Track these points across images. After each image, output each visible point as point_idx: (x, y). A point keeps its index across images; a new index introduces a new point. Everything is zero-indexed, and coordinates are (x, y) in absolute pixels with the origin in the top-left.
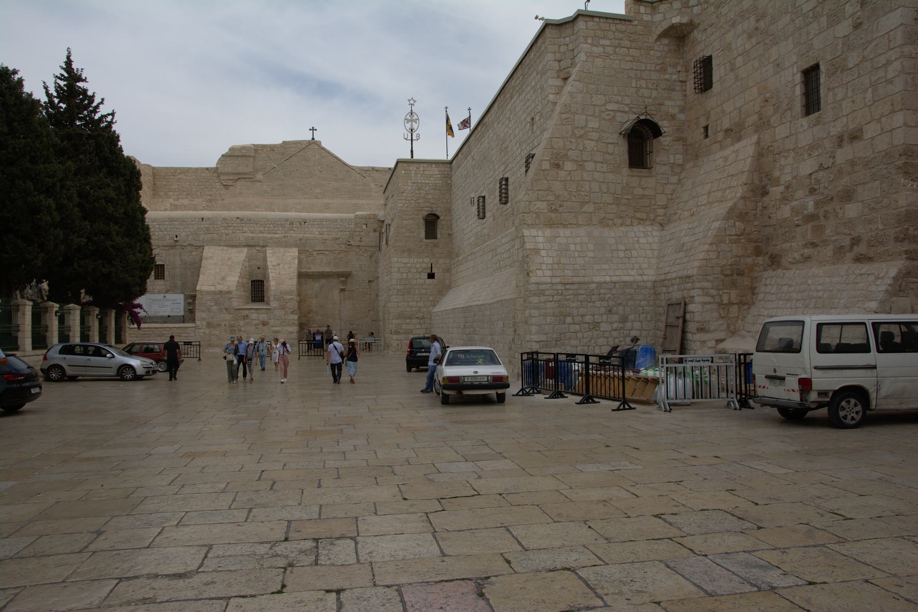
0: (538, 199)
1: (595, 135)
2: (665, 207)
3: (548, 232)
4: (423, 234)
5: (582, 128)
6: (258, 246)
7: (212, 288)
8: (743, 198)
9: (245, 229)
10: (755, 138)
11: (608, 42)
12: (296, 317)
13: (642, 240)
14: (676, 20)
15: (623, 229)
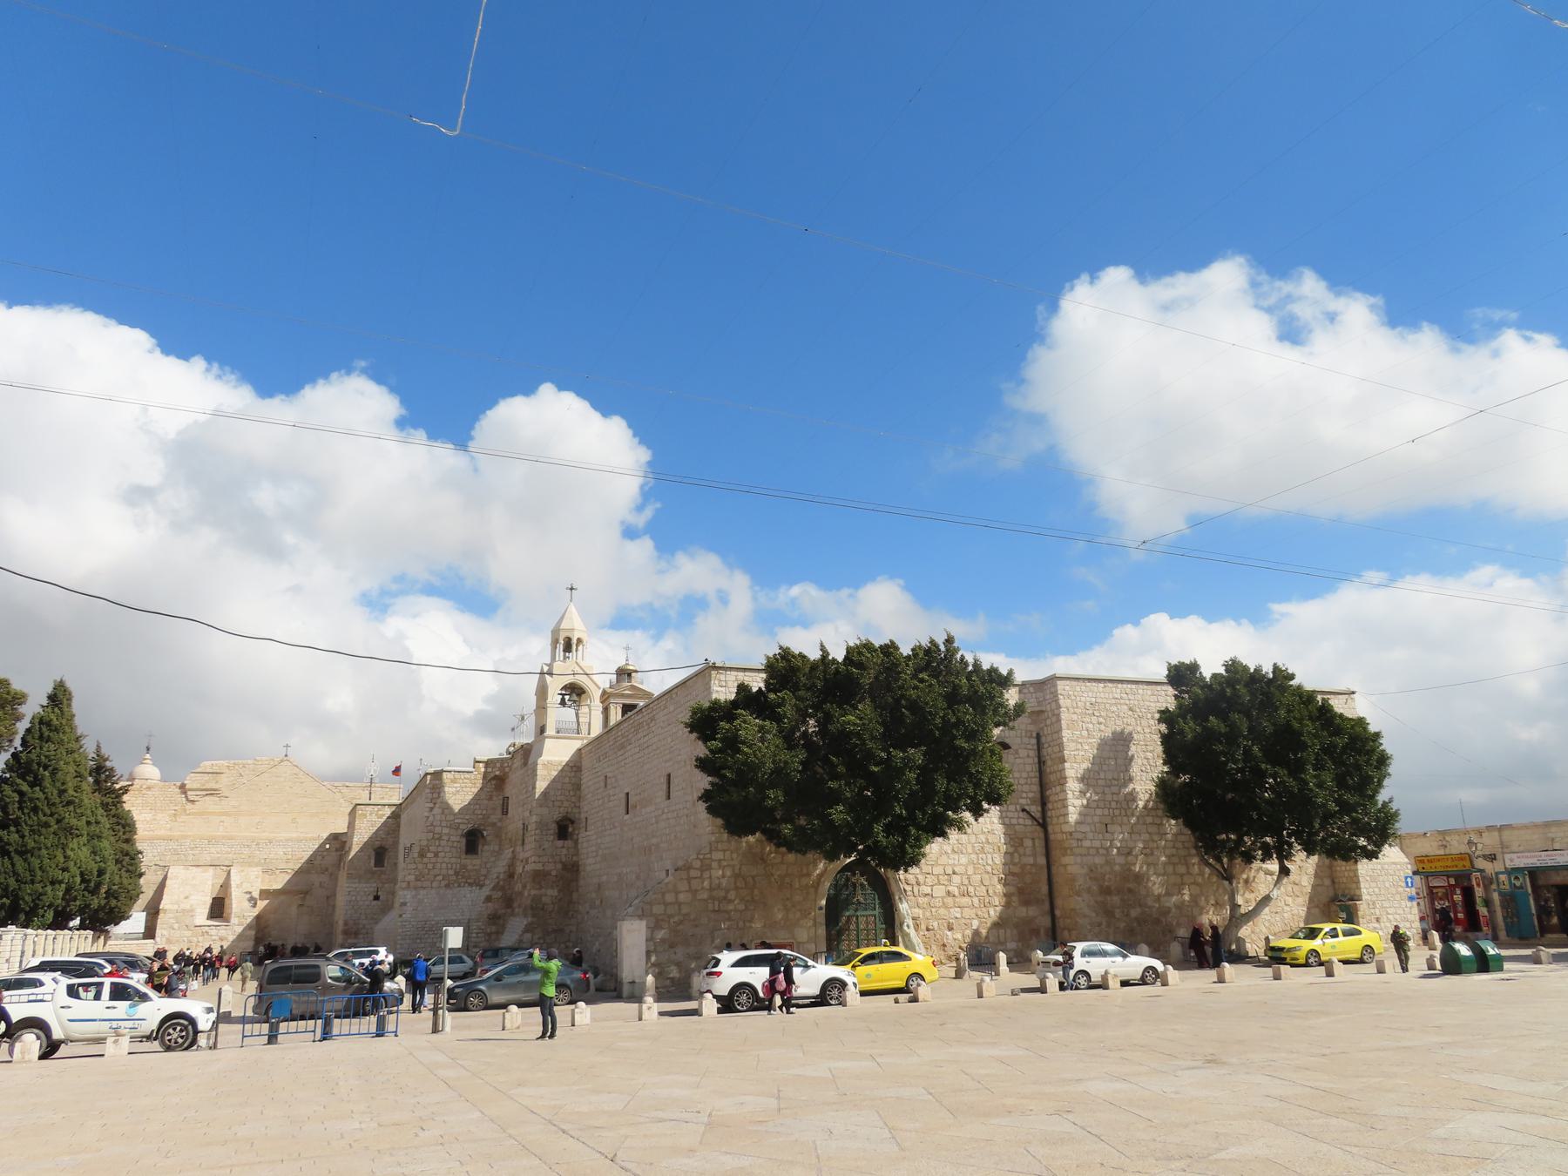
0: (409, 874)
1: (445, 838)
2: (485, 876)
3: (414, 893)
4: (373, 861)
5: (439, 834)
6: (223, 866)
7: (176, 907)
8: (504, 880)
9: (213, 850)
10: (512, 849)
11: (459, 785)
12: (253, 933)
13: (468, 895)
14: (497, 773)
15: (459, 889)
